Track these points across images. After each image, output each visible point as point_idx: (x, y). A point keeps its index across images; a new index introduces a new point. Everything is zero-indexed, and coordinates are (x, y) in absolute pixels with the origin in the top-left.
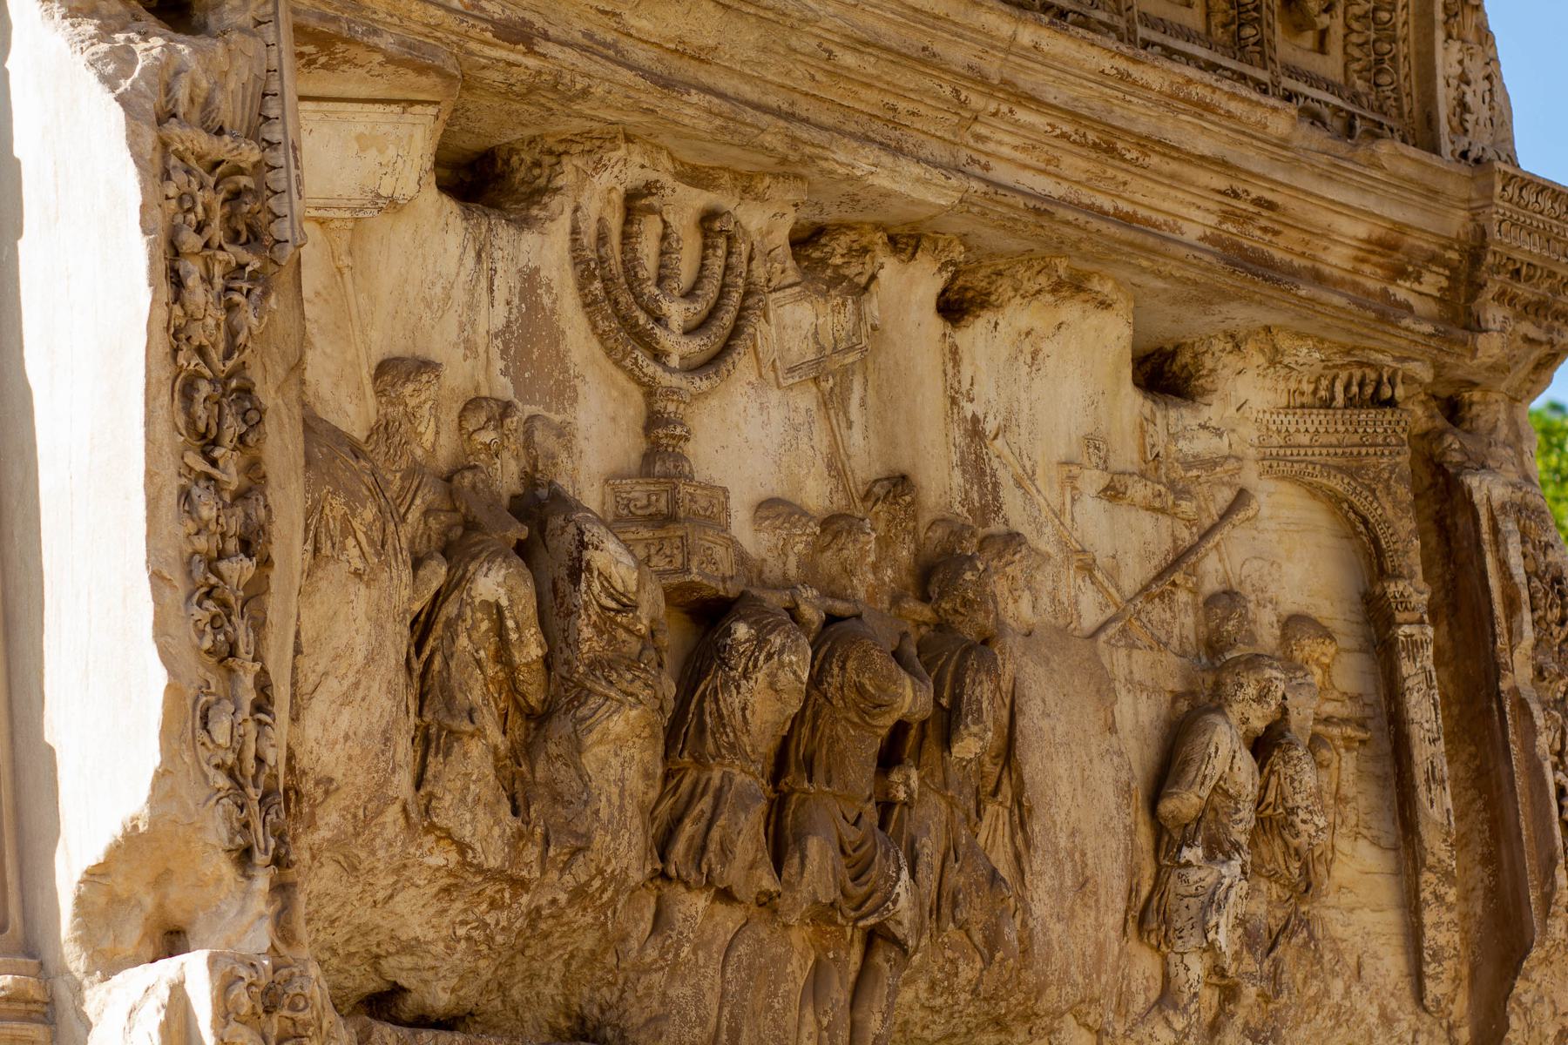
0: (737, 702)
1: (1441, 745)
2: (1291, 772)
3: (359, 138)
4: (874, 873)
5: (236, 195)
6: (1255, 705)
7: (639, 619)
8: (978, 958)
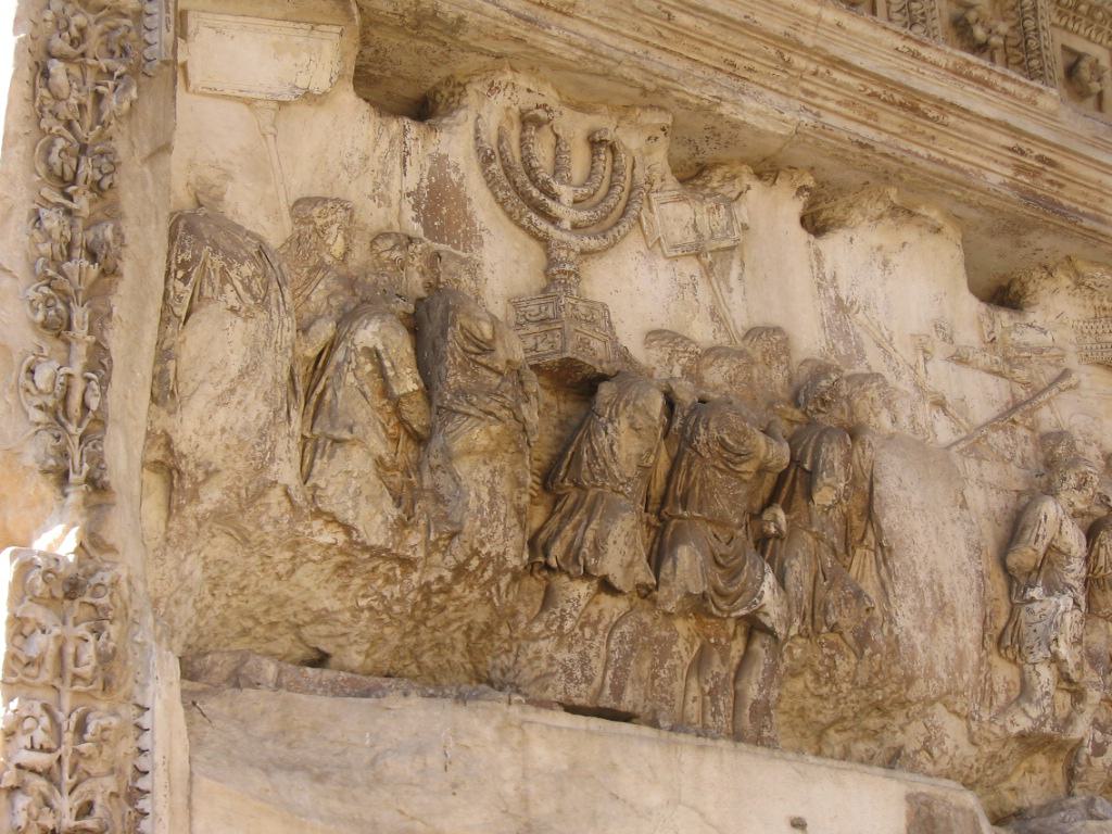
0: (606, 443)
4: (743, 577)
6: (1077, 492)
8: (852, 655)
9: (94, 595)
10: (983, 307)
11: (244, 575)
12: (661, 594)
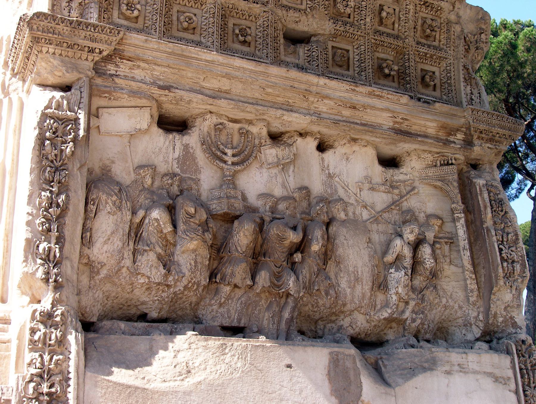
1: (467, 241)
3: (129, 116)
10: (384, 169)
11: (117, 294)
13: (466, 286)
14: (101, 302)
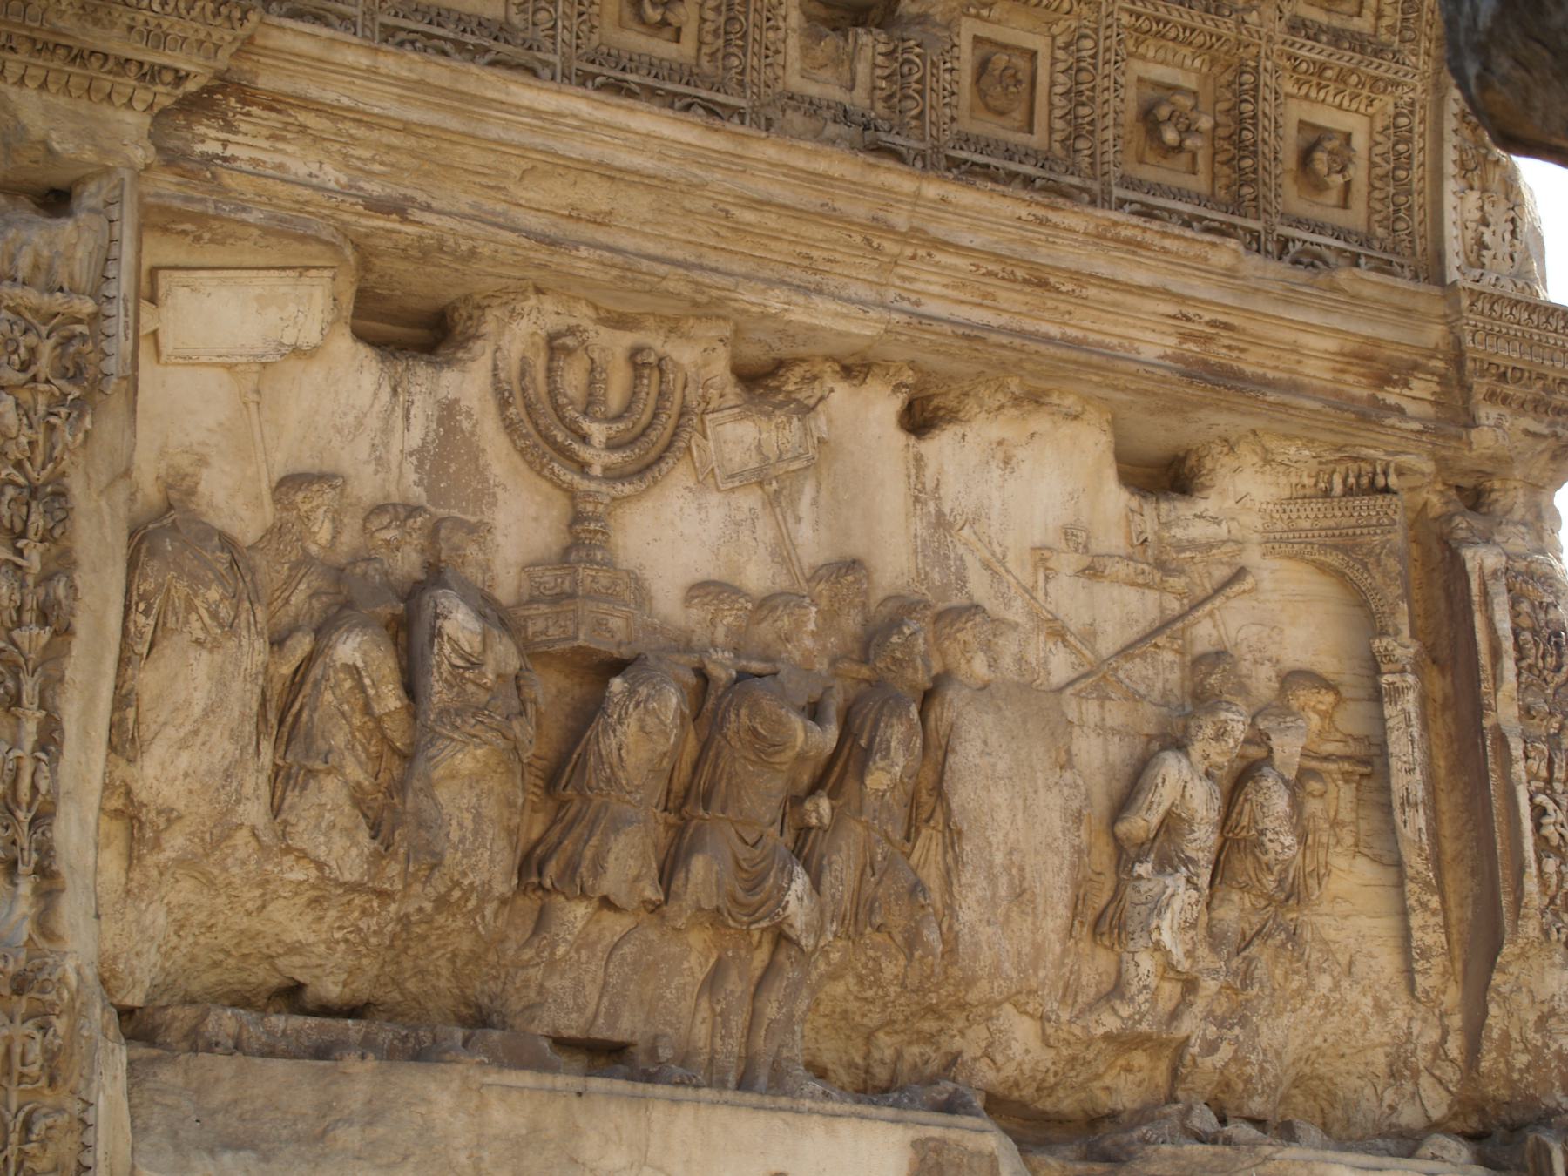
0: (614, 746)
1: (1418, 776)
2: (1261, 800)
3: (259, 298)
5: (70, 339)
7: (484, 675)
9: (43, 991)
10: (1135, 502)
11: (212, 914)
12: (671, 909)
13: (1406, 935)
14: (160, 940)
